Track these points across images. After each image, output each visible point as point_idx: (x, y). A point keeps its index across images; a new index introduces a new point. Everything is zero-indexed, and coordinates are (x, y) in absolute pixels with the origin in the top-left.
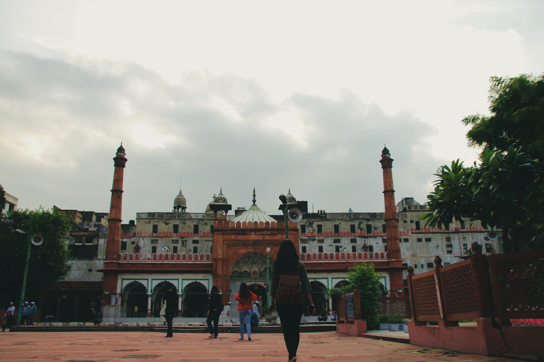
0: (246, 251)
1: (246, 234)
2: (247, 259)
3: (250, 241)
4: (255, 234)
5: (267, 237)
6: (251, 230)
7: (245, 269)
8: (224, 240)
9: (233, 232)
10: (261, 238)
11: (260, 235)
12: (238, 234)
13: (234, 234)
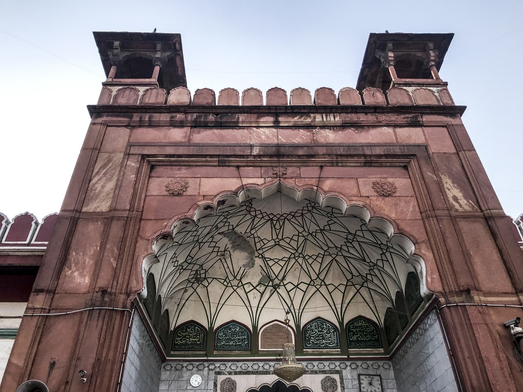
0: (232, 184)
1: (235, 126)
2: (239, 258)
3: (252, 146)
4: (277, 125)
5: (330, 136)
6: (258, 111)
7: (234, 311)
8: (130, 145)
9: (179, 116)
10: (300, 137)
11: (296, 127)
12: (197, 125)
13: (181, 125)
